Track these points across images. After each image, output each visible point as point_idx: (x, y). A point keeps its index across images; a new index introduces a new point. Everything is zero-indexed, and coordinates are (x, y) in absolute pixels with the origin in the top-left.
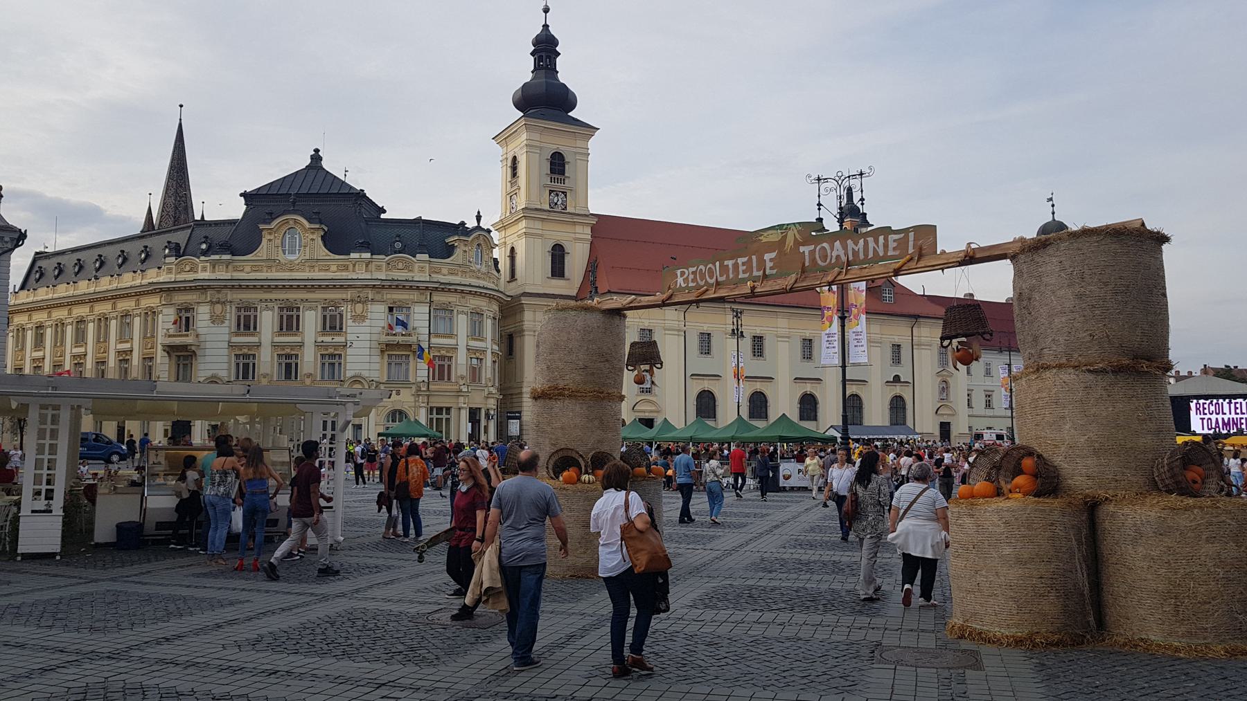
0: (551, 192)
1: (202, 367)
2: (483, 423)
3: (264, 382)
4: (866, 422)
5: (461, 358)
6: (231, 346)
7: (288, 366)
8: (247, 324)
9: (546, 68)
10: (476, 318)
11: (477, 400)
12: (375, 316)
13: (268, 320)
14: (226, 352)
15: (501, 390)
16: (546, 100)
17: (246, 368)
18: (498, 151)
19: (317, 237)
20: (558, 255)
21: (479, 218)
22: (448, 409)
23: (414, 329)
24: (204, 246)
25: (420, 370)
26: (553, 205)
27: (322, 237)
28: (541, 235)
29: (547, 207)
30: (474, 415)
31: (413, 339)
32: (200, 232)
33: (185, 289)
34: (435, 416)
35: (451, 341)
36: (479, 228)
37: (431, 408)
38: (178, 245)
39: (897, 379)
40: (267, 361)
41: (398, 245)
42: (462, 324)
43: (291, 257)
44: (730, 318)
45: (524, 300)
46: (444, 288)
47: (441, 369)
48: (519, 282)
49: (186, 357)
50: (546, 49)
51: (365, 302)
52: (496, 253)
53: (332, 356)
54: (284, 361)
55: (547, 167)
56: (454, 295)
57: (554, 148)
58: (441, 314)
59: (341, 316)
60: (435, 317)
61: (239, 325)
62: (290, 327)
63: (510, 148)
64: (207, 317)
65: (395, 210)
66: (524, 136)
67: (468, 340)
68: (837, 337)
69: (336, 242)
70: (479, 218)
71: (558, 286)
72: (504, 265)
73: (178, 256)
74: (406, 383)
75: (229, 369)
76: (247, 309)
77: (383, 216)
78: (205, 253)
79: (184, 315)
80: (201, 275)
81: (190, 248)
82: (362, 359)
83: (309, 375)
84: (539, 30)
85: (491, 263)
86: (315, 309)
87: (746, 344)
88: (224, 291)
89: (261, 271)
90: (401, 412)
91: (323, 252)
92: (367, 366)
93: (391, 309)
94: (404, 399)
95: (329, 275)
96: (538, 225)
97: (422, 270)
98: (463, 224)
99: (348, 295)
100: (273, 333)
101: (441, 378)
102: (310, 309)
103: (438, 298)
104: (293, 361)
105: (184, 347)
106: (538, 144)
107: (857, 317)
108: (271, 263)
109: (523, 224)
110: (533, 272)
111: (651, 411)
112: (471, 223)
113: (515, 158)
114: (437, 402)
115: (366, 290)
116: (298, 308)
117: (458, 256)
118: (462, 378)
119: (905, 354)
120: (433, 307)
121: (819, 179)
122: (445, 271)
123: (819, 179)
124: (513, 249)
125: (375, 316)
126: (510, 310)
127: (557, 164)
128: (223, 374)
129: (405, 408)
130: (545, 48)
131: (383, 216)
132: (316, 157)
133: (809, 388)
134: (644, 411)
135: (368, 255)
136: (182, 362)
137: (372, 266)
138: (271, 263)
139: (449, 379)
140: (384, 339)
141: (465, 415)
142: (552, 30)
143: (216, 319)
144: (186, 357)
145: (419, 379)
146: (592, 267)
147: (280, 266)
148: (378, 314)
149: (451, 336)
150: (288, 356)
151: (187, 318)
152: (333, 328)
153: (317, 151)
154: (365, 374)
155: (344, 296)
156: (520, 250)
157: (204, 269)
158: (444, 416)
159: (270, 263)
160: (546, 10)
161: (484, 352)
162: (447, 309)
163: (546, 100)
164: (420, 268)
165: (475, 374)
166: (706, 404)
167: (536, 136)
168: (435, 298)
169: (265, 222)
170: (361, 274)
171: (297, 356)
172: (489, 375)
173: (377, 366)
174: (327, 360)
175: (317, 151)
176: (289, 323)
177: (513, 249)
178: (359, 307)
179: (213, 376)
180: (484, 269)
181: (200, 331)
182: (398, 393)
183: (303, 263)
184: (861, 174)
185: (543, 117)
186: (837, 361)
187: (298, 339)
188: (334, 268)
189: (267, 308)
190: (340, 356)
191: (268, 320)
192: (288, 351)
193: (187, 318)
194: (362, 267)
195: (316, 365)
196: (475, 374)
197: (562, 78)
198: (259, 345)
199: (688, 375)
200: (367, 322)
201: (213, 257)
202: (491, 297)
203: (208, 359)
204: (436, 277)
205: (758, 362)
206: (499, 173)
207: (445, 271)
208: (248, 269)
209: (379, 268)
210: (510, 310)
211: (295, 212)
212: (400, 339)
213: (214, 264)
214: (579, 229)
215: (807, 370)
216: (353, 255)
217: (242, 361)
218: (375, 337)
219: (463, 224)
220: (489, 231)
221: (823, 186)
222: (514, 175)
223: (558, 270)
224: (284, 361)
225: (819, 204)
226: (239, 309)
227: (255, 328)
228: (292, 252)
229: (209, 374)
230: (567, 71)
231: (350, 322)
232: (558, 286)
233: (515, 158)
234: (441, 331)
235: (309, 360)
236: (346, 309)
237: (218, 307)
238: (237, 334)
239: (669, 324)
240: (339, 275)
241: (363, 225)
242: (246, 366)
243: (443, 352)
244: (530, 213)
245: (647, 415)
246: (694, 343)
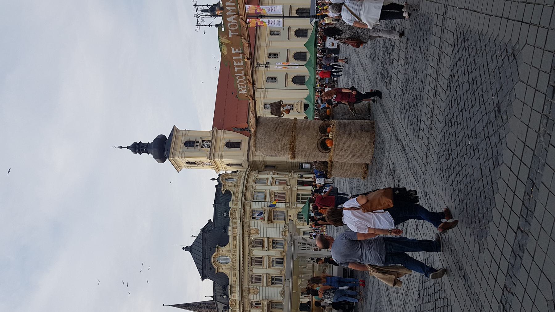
1: (276, 299)
2: (304, 179)
3: (283, 272)
4: (309, 7)
5: (276, 188)
6: (268, 286)
7: (277, 262)
8: (258, 279)
9: (147, 148)
10: (258, 181)
11: (294, 182)
12: (256, 225)
13: (257, 270)
14: (270, 288)
15: (290, 171)
16: (161, 148)
17: (277, 280)
18: (184, 170)
19: (221, 249)
20: (230, 145)
21: (214, 179)
22: (298, 194)
23: (262, 208)
24: (225, 297)
25: (280, 206)
27: (222, 246)
28: (222, 152)
29: (209, 149)
30: (300, 183)
31: (267, 209)
32: (219, 298)
33: (243, 305)
34: (300, 200)
35: (268, 192)
36: (218, 179)
37: (297, 202)
38: (224, 308)
40: (274, 271)
41: (225, 214)
42: (260, 188)
43: (230, 260)
44: (260, 68)
45: (250, 160)
46: (244, 195)
47: (280, 197)
48: (242, 162)
49: (272, 305)
50: (138, 148)
51: (250, 229)
52: (229, 172)
53: (273, 243)
54: (275, 264)
56: (247, 190)
57: (183, 146)
58: (256, 196)
59: (256, 239)
60: (257, 199)
61: (259, 283)
62: (260, 261)
63: (182, 164)
64: (255, 296)
65: (210, 215)
66: (177, 158)
67: (268, 185)
68: (271, 20)
69: (224, 241)
70: (214, 179)
71: (245, 145)
72: (235, 169)
73: (229, 307)
74: (286, 212)
75: (278, 287)
76: (252, 279)
77: (212, 221)
78: (228, 296)
79: (254, 305)
80: (237, 298)
81: (225, 302)
82: (274, 231)
83: (281, 253)
84: (129, 151)
85: (234, 174)
86: (253, 250)
87: (272, 61)
88: (244, 288)
89: (236, 273)
90: (298, 215)
91: (228, 247)
92: (278, 229)
93: (253, 218)
94: (293, 213)
95: (238, 244)
96: (217, 153)
97: (236, 205)
98: (216, 186)
99: (246, 236)
100: (262, 268)
101: (284, 197)
102: (252, 252)
103: (249, 197)
104: (275, 260)
105: (268, 305)
107: (261, 9)
108: (232, 268)
109: (216, 160)
110: (238, 156)
111: (301, 105)
112: (216, 183)
113: (188, 163)
114: (294, 199)
115: (245, 229)
116: (252, 257)
117: (231, 189)
121: (198, 25)
122: (237, 195)
123: (198, 25)
124: (227, 165)
125: (256, 225)
126: (254, 167)
127: (190, 144)
128: (280, 290)
129: (296, 213)
130: (138, 148)
131: (212, 221)
132: (186, 249)
133: (292, 33)
135: (229, 228)
136: (274, 306)
137: (234, 226)
138: (232, 268)
139: (284, 194)
140: (266, 221)
141: (301, 187)
142: (130, 145)
143: (256, 292)
144: (272, 305)
145: (284, 207)
146: (236, 130)
147: (234, 264)
148: (255, 224)
149: (265, 193)
150: (273, 262)
151: (256, 304)
152: (261, 243)
153: (183, 248)
154: (281, 230)
155: (247, 238)
156: (227, 162)
157: (235, 297)
158: (301, 196)
159: (232, 269)
160: (121, 147)
161: (273, 178)
162: (254, 194)
163: (161, 148)
164: (235, 205)
165: (282, 182)
166: (299, 80)
167: (177, 153)
168: (249, 199)
169: (215, 271)
170: (238, 231)
171: (273, 259)
172: (283, 176)
173: (278, 224)
174: (275, 246)
175: (183, 248)
176: (258, 261)
177: (227, 165)
178: (252, 232)
179: (281, 294)
180: (236, 178)
181: (261, 299)
182: (290, 216)
183: (233, 255)
184: (196, 6)
185: (169, 150)
186: (281, 20)
187: (265, 258)
188: (235, 242)
189: (252, 270)
190: (273, 240)
191: (257, 270)
192: (270, 262)
193: (256, 304)
194: (235, 230)
195: (276, 251)
196: (282, 182)
197: (151, 141)
198: (268, 274)
199: (285, 88)
200: (259, 228)
201: (229, 293)
202: (249, 175)
203: (273, 296)
204: (240, 198)
205: (280, 56)
206: (194, 170)
207: (237, 195)
208: (235, 278)
209: (235, 223)
210: (254, 167)
211: (210, 258)
212: (267, 215)
213: (232, 292)
214: (219, 135)
215: (284, 33)
216: (229, 234)
217: (274, 282)
218: (265, 225)
219: (216, 186)
220: (220, 175)
221: (201, 24)
222: (194, 163)
223: (237, 145)
224: (275, 264)
225: (209, 26)
226: (252, 282)
227: (260, 276)
228: (228, 260)
229: (279, 295)
230: (148, 139)
231: (259, 236)
232: (245, 145)
233: (187, 163)
234: (263, 197)
235: (275, 253)
236: (253, 237)
237: (251, 291)
238: (263, 283)
239: (262, 96)
240: (238, 240)
241: (216, 229)
242: (276, 280)
243: (273, 196)
244: (211, 157)
245: (303, 107)
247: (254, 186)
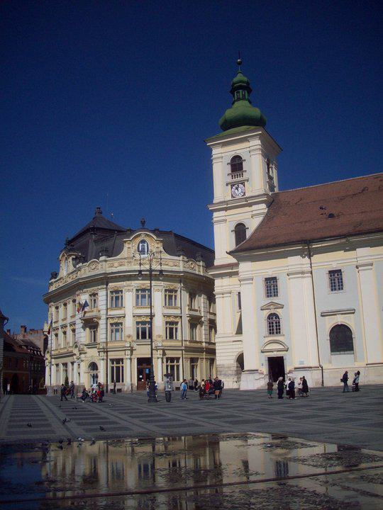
34: (115, 365)
37: (112, 361)
55: (228, 169)
57: (233, 154)
96: (223, 213)
106: (219, 155)
114: (112, 355)
118: (129, 336)
134: (271, 351)
158: (121, 365)
199: (318, 314)
207: (116, 264)
214: (254, 207)
243: (116, 321)
246: (325, 281)
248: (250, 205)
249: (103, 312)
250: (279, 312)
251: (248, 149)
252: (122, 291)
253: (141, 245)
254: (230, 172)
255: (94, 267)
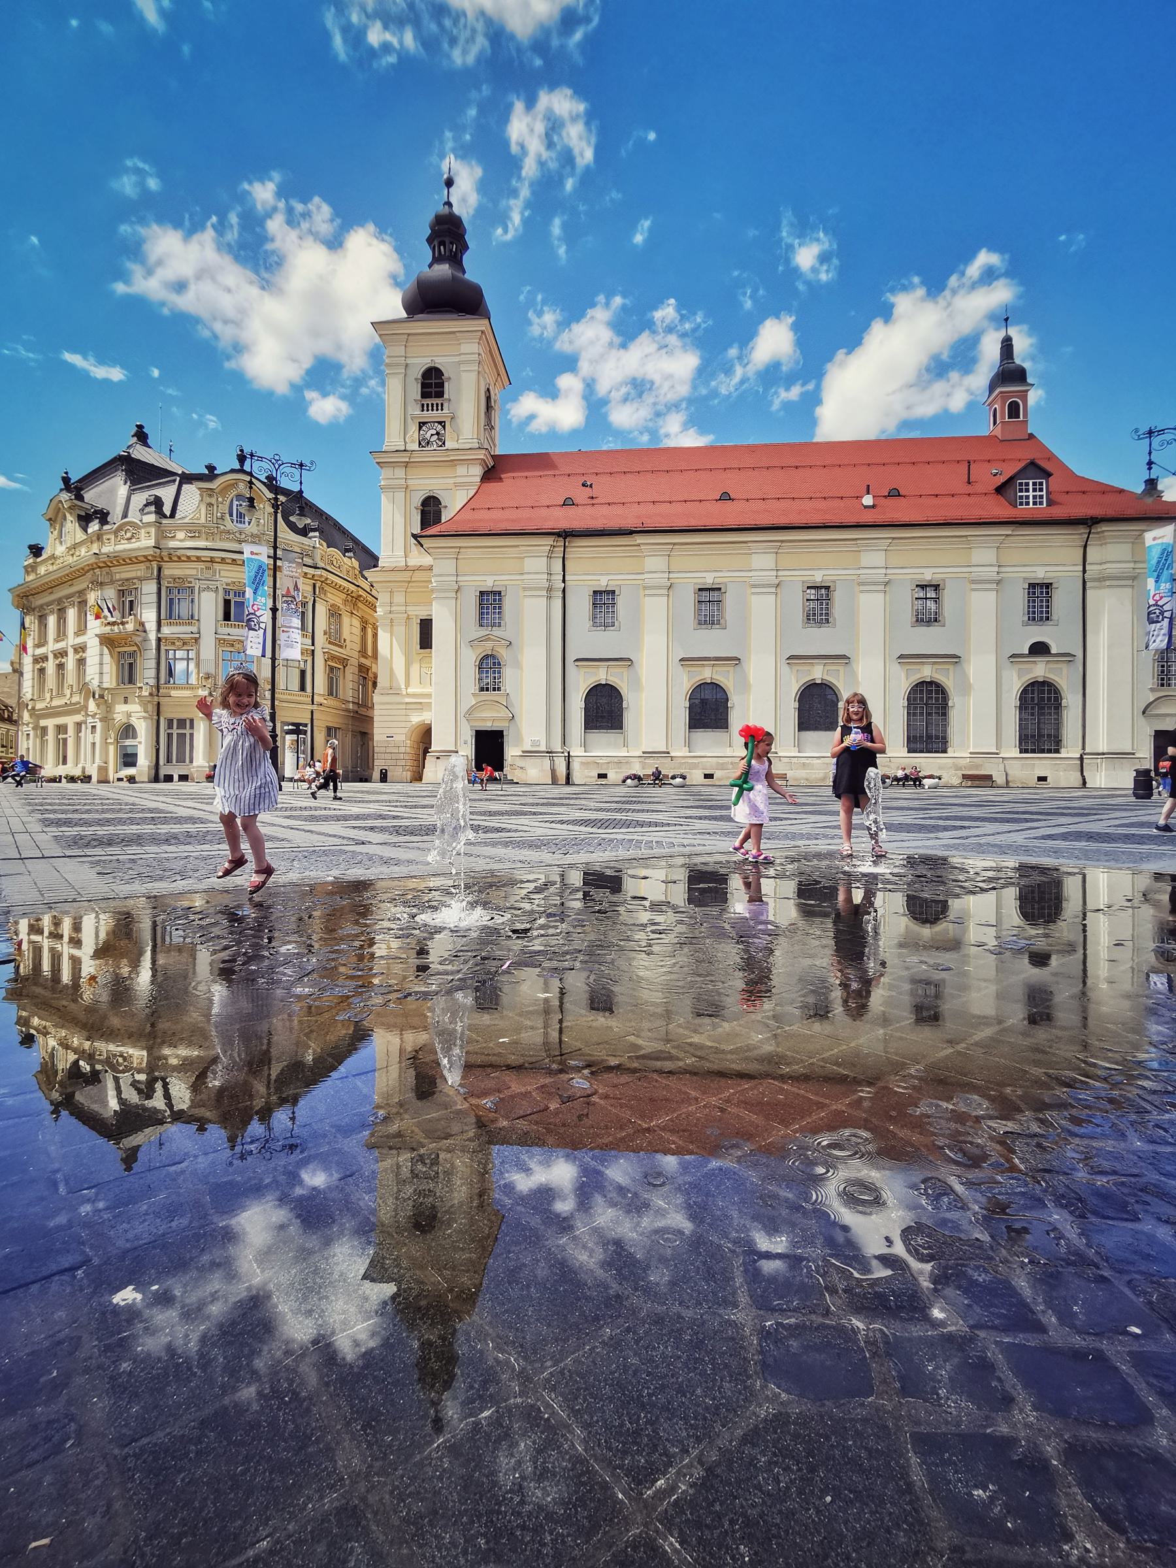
0: (421, 425)
26: (423, 443)
34: (175, 732)
37: (170, 722)
39: (1039, 649)
55: (416, 390)
96: (400, 472)
119: (1064, 602)
120: (165, 583)
129: (134, 721)
134: (483, 720)
158: (187, 731)
168: (166, 572)
175: (140, 427)
189: (52, 612)
214: (461, 470)
245: (488, 726)
247: (212, 584)
248: (453, 463)
249: (151, 626)
250: (503, 653)
251: (457, 359)
252: (192, 589)
253: (235, 503)
254: (419, 397)
255: (129, 535)
